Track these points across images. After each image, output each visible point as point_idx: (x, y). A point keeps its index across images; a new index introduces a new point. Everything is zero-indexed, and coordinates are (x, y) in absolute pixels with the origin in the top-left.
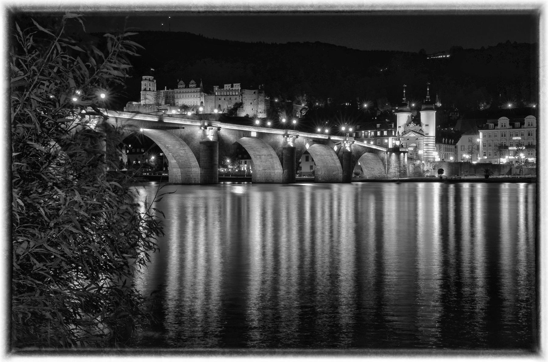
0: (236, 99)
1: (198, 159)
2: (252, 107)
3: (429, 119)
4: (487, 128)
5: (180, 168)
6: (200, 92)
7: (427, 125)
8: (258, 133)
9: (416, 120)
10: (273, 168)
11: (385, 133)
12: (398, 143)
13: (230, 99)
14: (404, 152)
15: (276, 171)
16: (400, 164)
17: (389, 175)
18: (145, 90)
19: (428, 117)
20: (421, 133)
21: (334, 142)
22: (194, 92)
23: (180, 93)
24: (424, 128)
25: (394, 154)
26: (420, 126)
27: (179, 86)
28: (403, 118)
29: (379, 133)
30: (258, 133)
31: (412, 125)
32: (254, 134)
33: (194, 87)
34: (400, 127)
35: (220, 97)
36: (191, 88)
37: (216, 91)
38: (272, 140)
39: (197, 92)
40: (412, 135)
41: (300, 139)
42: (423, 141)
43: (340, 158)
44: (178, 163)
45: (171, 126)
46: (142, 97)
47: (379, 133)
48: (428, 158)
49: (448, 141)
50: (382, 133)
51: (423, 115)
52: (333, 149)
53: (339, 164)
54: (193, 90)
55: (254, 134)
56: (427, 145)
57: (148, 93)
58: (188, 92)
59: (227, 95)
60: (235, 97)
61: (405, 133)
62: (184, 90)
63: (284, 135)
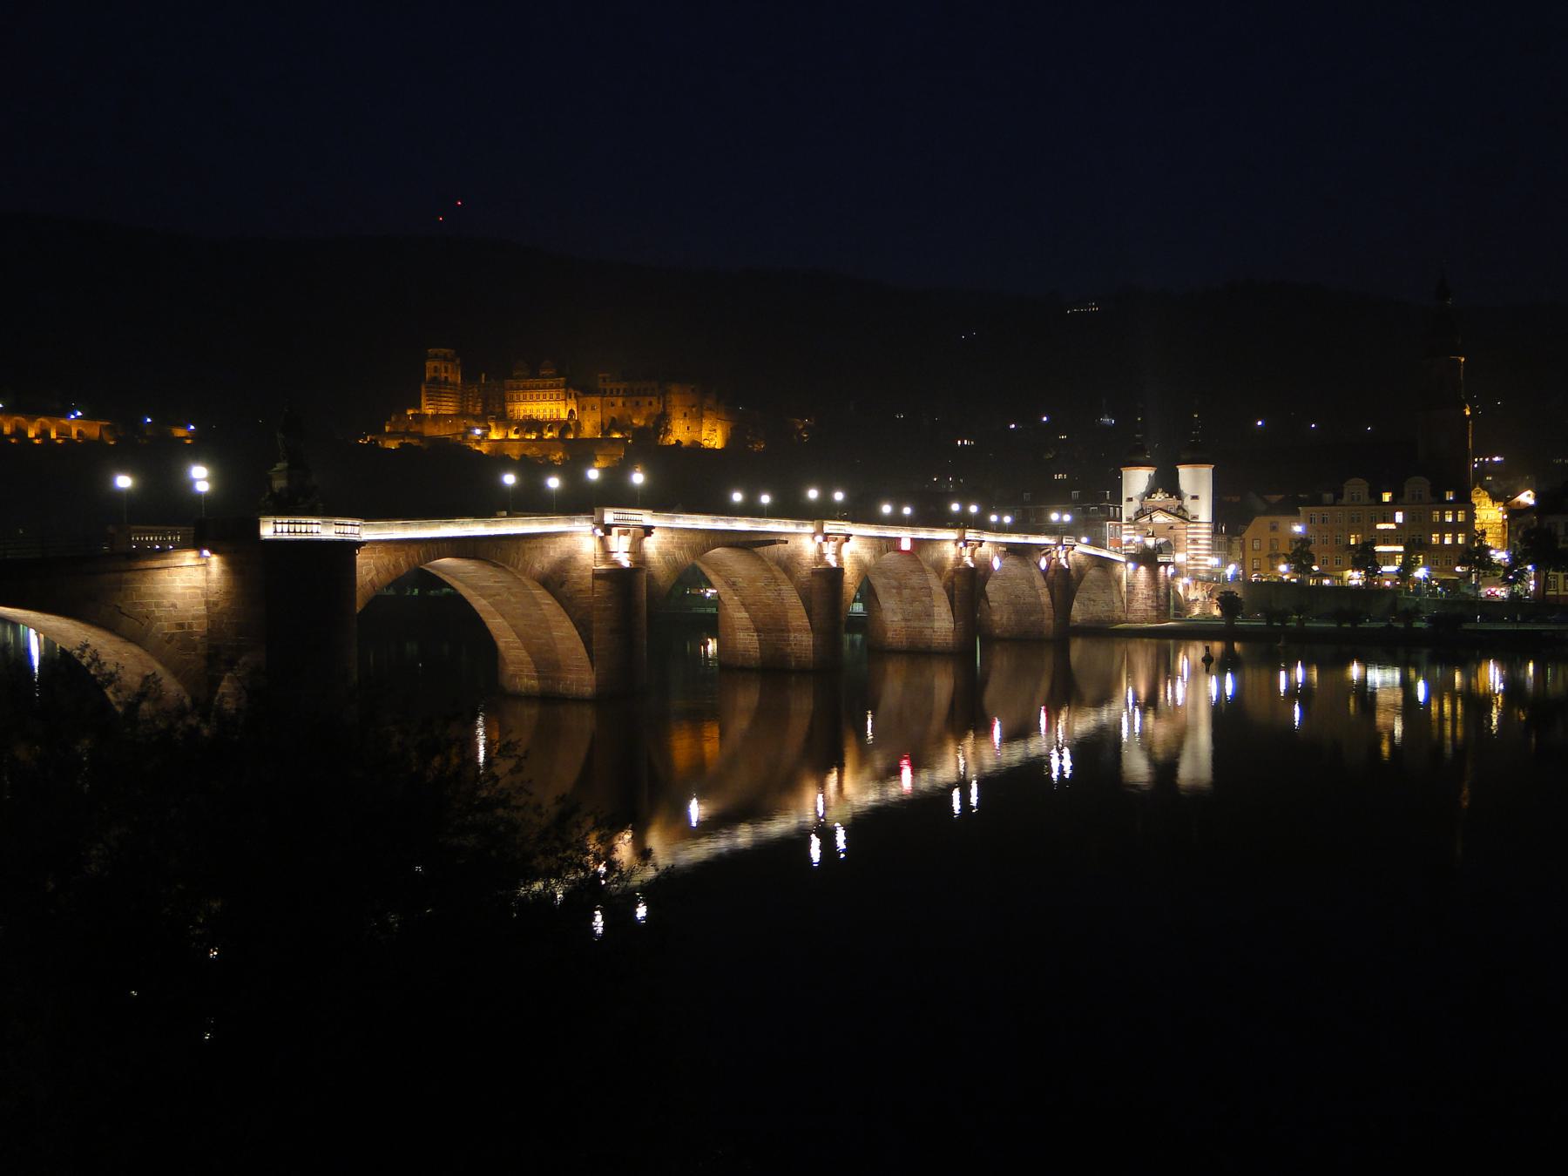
1: (809, 612)
3: (1196, 481)
4: (1316, 502)
5: (757, 630)
6: (567, 386)
7: (1195, 497)
8: (913, 540)
9: (1167, 483)
10: (929, 615)
12: (1150, 542)
14: (1166, 564)
15: (937, 625)
16: (1157, 590)
17: (1130, 616)
19: (1196, 480)
20: (1181, 514)
21: (1040, 548)
22: (551, 387)
23: (518, 389)
24: (1187, 502)
25: (1142, 568)
26: (1180, 498)
28: (1137, 480)
30: (913, 540)
31: (1159, 497)
32: (906, 545)
33: (551, 377)
34: (1130, 500)
36: (543, 377)
38: (936, 555)
39: (557, 387)
40: (1160, 518)
41: (986, 549)
42: (1184, 532)
43: (1050, 585)
44: (753, 619)
45: (761, 538)
48: (1196, 571)
51: (1185, 474)
52: (1038, 565)
53: (1045, 598)
54: (549, 382)
55: (906, 545)
56: (1194, 541)
61: (1141, 513)
62: (528, 383)
63: (956, 542)
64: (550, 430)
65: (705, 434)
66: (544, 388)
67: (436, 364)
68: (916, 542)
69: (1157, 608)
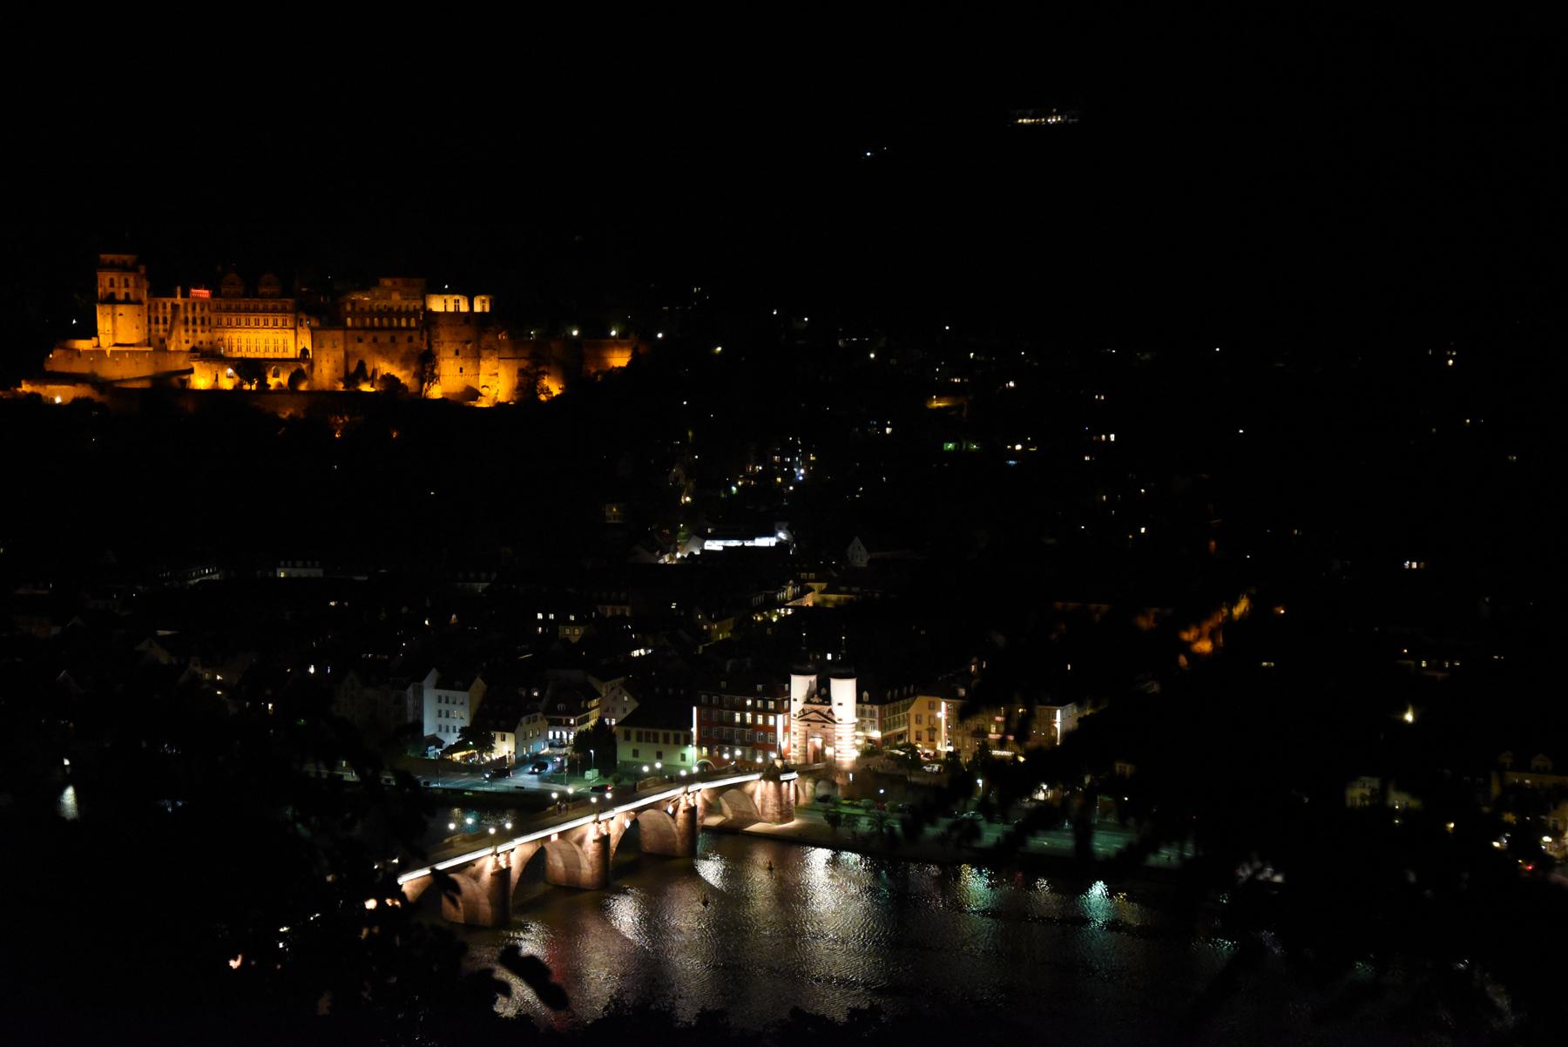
0: (410, 340)
2: (460, 363)
3: (844, 691)
11: (771, 705)
13: (393, 339)
18: (111, 300)
21: (668, 800)
22: (274, 310)
23: (228, 310)
24: (834, 707)
25: (771, 783)
27: (223, 290)
28: (800, 686)
29: (759, 704)
32: (554, 838)
33: (272, 296)
35: (361, 334)
36: (263, 296)
37: (348, 314)
39: (284, 311)
46: (103, 324)
47: (759, 704)
49: (900, 693)
50: (765, 704)
54: (270, 305)
57: (121, 309)
58: (255, 310)
59: (381, 328)
60: (408, 334)
64: (276, 375)
65: (483, 380)
66: (265, 310)
67: (114, 276)
68: (561, 834)
69: (780, 813)
